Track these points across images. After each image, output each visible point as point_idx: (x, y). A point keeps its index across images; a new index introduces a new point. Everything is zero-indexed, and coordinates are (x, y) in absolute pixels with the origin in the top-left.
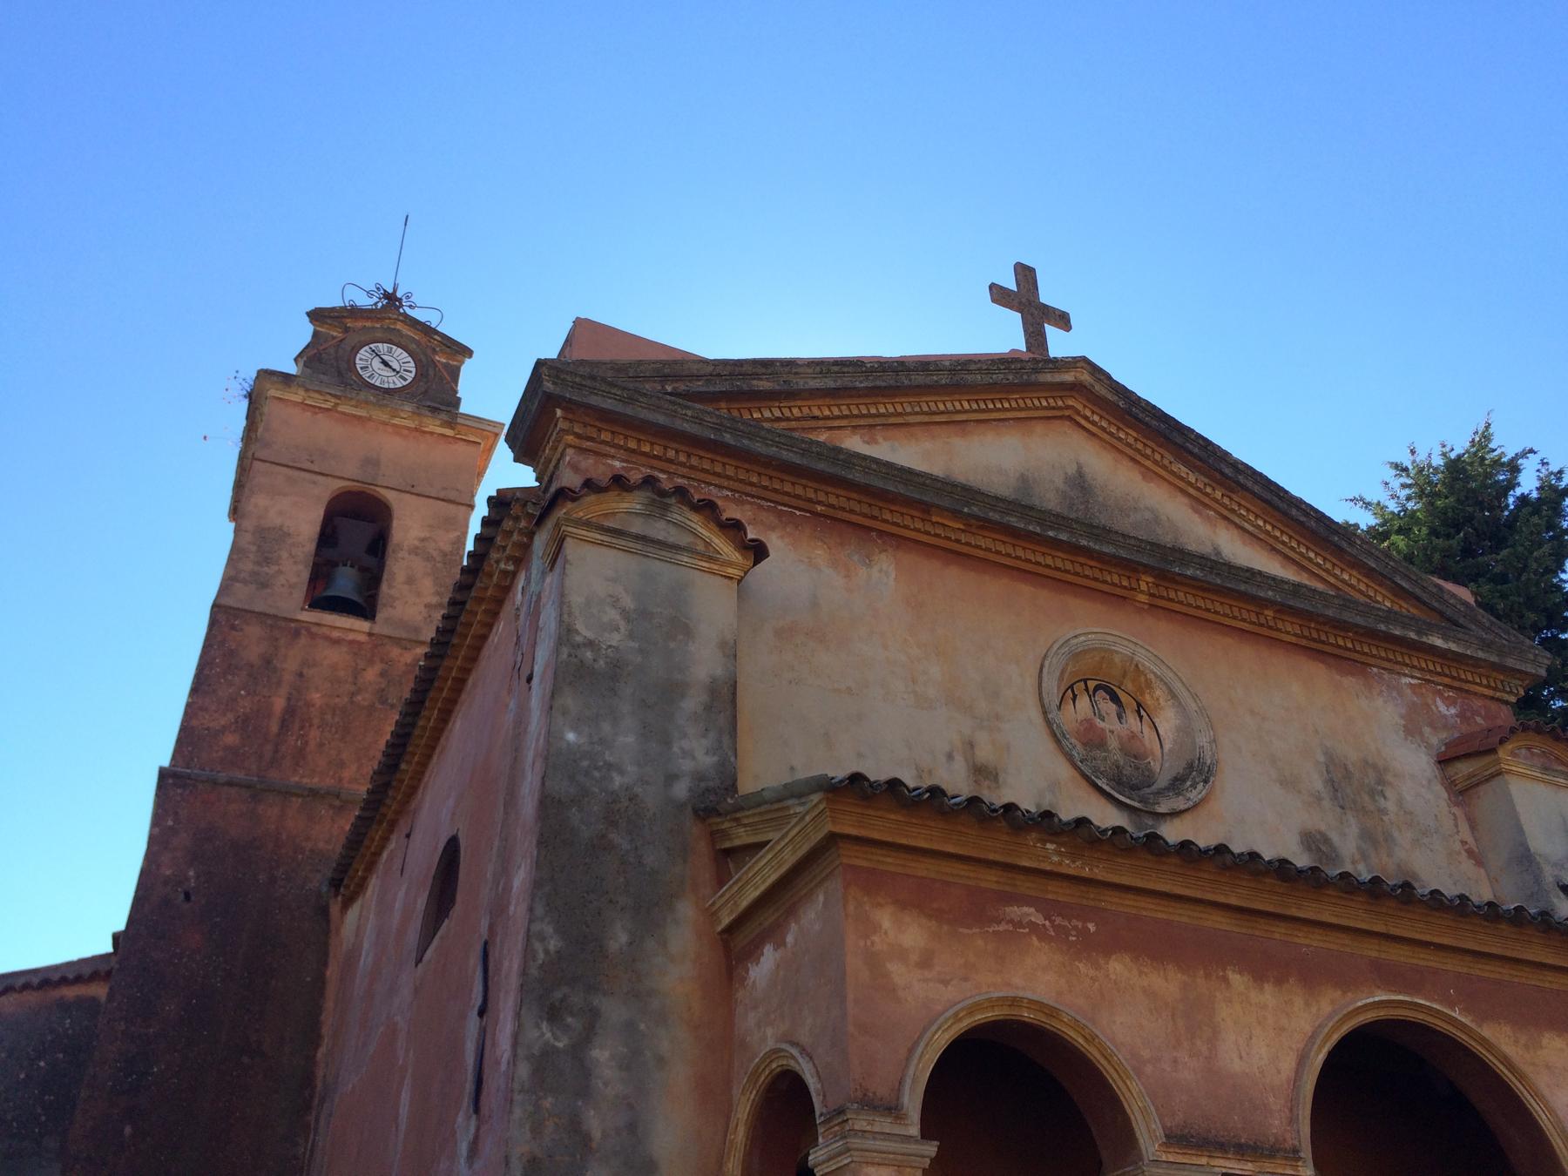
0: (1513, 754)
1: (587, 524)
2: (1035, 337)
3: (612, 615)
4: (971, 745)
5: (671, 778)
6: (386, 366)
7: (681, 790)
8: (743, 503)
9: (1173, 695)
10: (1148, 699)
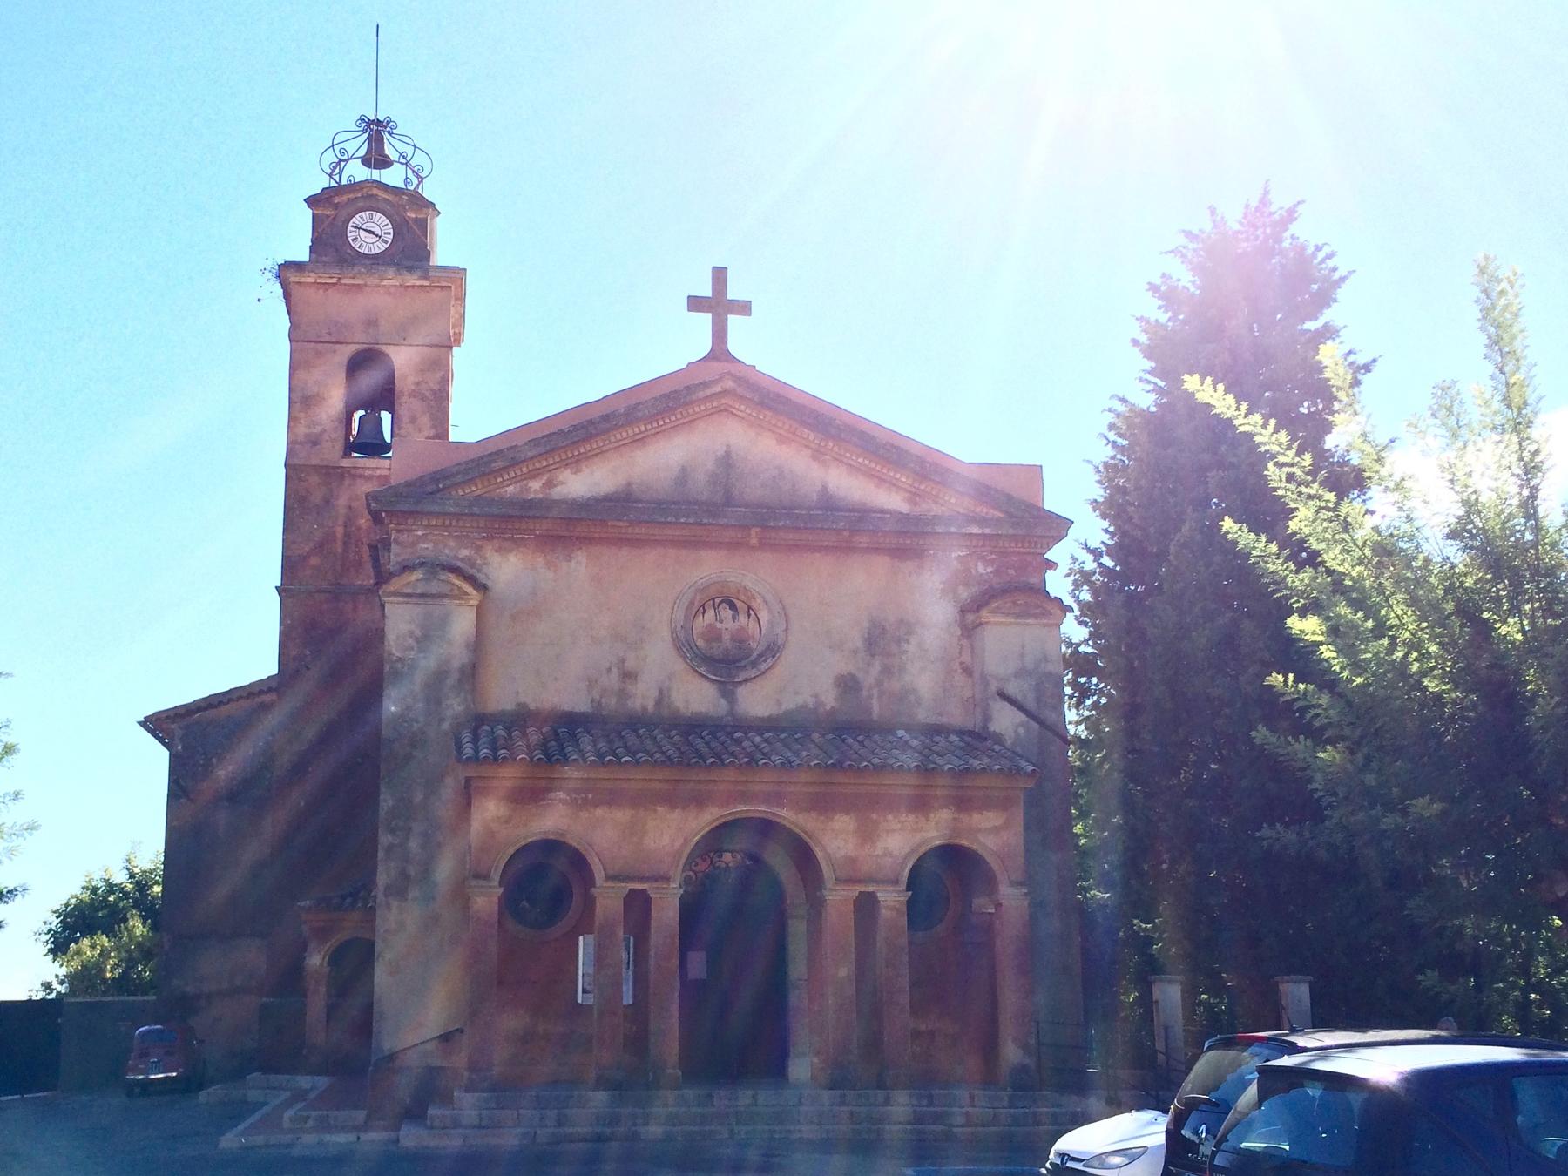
0: (994, 612)
1: (395, 594)
2: (720, 334)
3: (411, 641)
4: (623, 661)
5: (442, 720)
6: (371, 233)
7: (446, 726)
8: (493, 538)
9: (765, 602)
10: (753, 604)
